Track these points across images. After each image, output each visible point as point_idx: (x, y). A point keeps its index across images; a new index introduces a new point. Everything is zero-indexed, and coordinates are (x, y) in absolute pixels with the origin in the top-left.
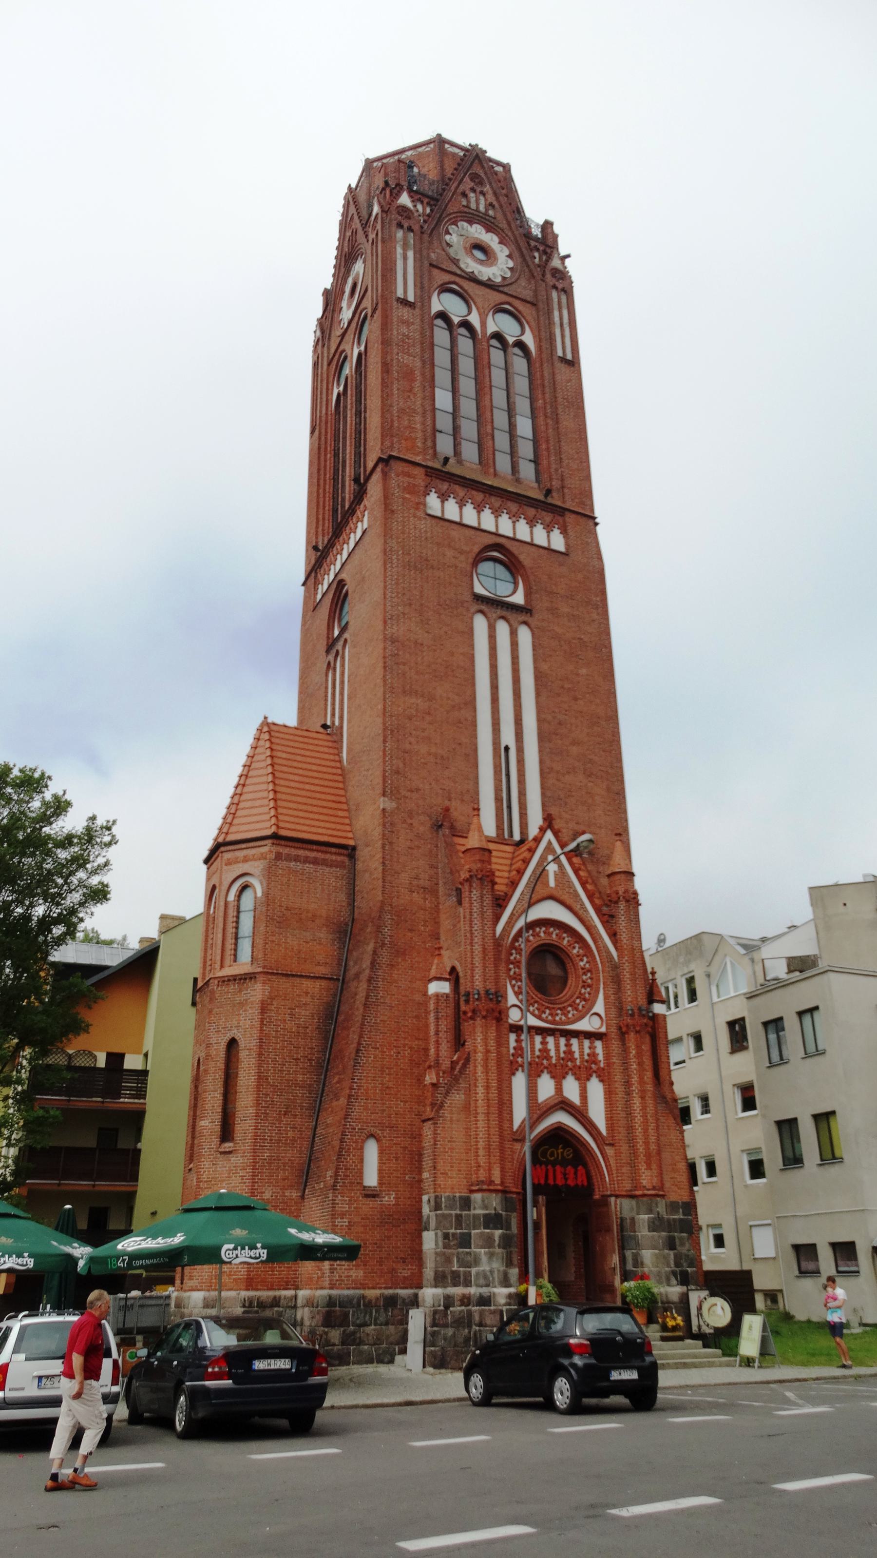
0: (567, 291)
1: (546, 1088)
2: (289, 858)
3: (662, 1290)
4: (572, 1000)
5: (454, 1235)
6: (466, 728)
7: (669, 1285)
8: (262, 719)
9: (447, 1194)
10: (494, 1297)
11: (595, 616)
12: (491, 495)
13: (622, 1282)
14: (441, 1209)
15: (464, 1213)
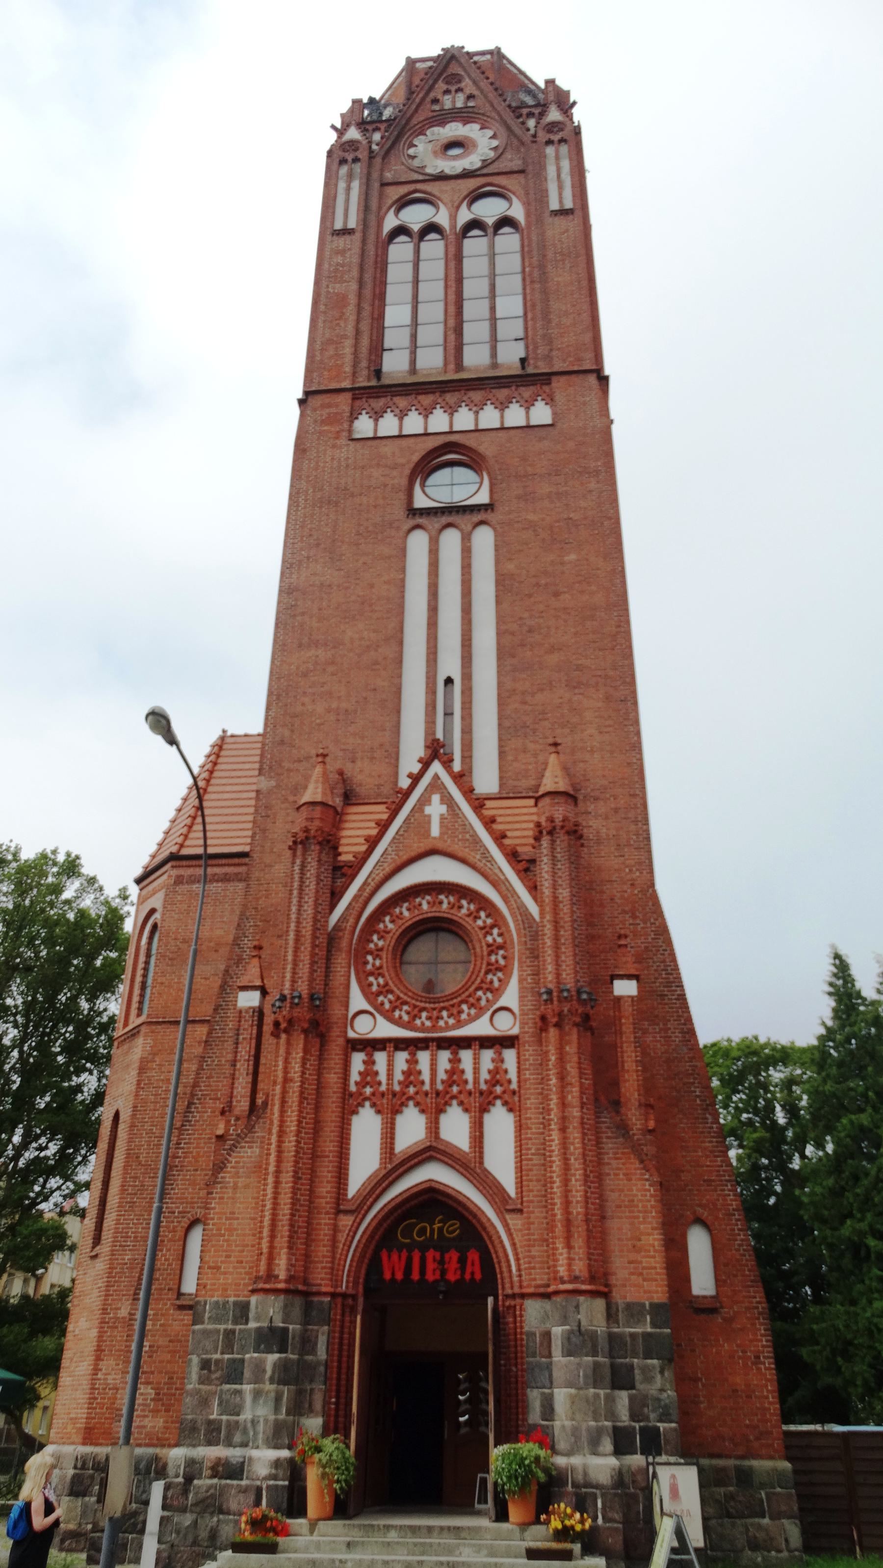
0: (572, 138)
1: (411, 1129)
2: (193, 880)
3: (576, 1461)
4: (467, 993)
5: (217, 1361)
6: (385, 669)
7: (595, 1453)
8: (221, 733)
9: (215, 1299)
10: (249, 1465)
11: (593, 485)
12: (444, 392)
13: (495, 1446)
14: (203, 1323)
15: (238, 1327)
